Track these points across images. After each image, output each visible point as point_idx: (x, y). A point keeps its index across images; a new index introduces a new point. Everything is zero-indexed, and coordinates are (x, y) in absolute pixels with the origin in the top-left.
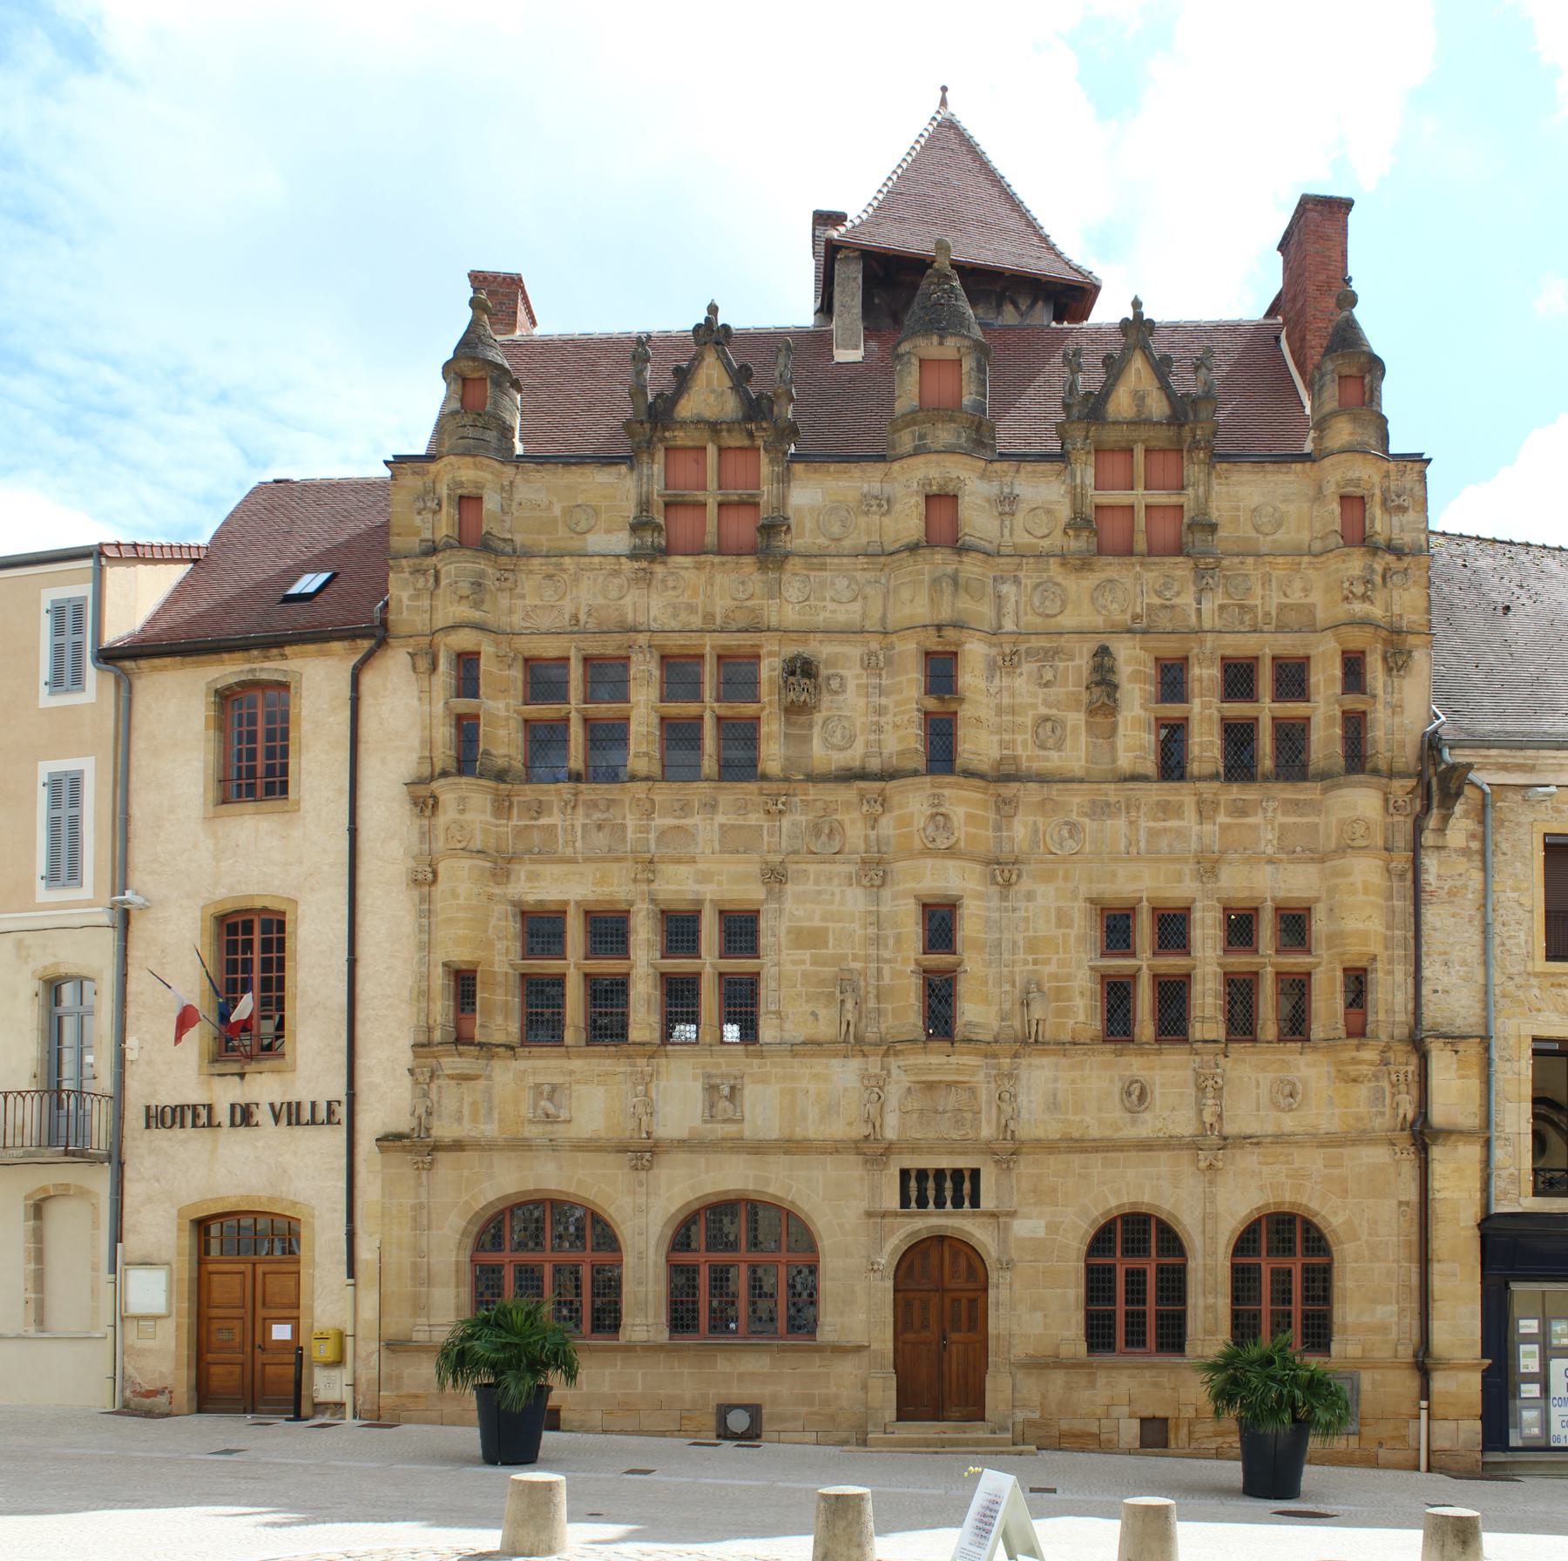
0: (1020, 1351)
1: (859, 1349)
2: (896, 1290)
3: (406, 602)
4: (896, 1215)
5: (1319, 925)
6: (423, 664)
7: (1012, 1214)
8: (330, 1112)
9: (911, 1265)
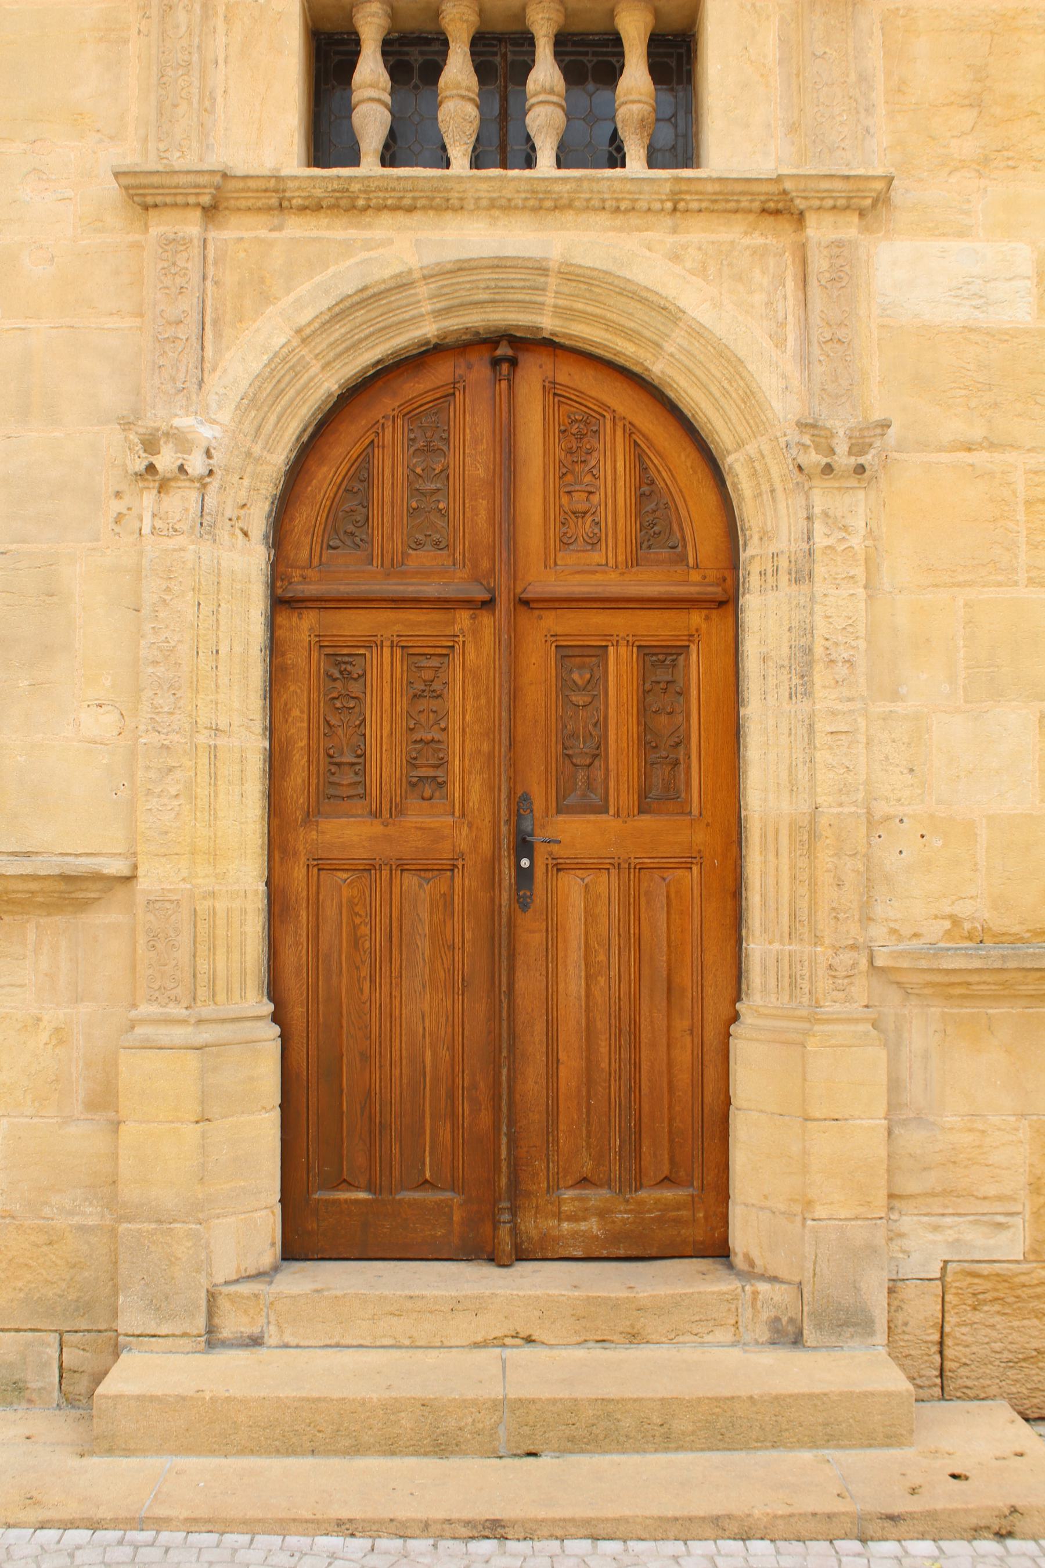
0: (920, 905)
1: (73, 892)
2: (281, 603)
4: (277, 200)
7: (868, 202)
9: (361, 478)
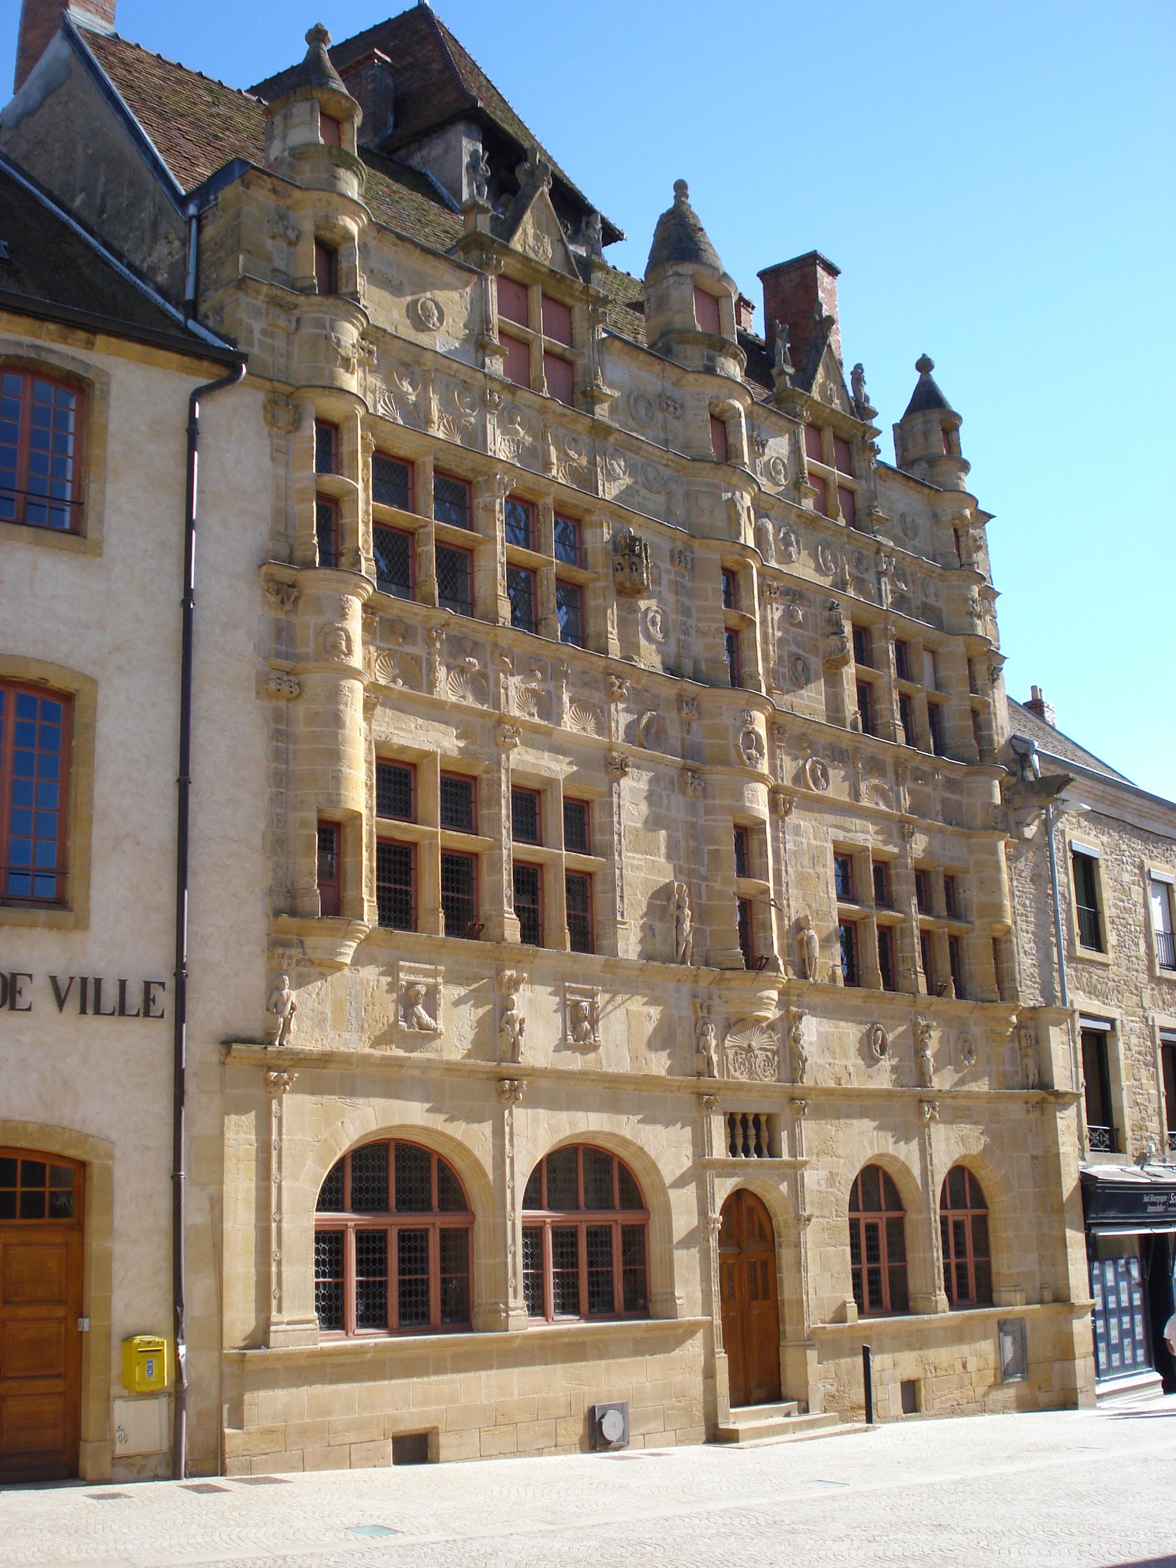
3: (257, 335)
5: (971, 894)
6: (284, 416)
8: (148, 1000)
